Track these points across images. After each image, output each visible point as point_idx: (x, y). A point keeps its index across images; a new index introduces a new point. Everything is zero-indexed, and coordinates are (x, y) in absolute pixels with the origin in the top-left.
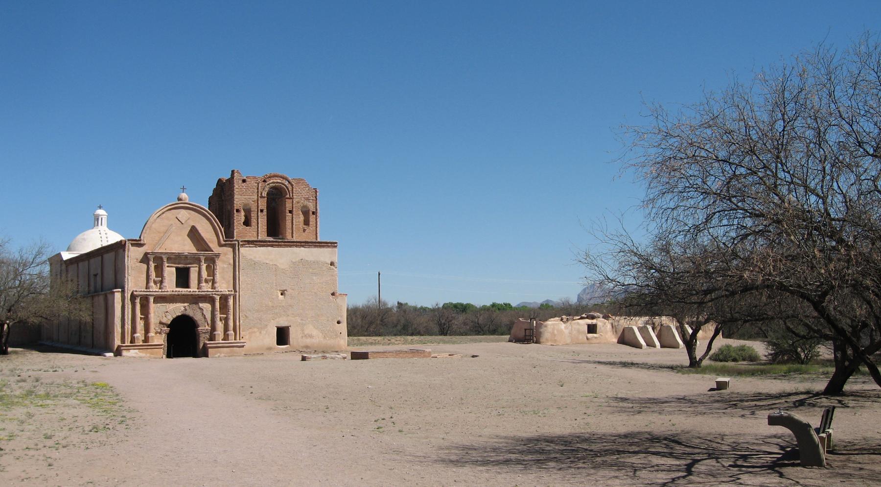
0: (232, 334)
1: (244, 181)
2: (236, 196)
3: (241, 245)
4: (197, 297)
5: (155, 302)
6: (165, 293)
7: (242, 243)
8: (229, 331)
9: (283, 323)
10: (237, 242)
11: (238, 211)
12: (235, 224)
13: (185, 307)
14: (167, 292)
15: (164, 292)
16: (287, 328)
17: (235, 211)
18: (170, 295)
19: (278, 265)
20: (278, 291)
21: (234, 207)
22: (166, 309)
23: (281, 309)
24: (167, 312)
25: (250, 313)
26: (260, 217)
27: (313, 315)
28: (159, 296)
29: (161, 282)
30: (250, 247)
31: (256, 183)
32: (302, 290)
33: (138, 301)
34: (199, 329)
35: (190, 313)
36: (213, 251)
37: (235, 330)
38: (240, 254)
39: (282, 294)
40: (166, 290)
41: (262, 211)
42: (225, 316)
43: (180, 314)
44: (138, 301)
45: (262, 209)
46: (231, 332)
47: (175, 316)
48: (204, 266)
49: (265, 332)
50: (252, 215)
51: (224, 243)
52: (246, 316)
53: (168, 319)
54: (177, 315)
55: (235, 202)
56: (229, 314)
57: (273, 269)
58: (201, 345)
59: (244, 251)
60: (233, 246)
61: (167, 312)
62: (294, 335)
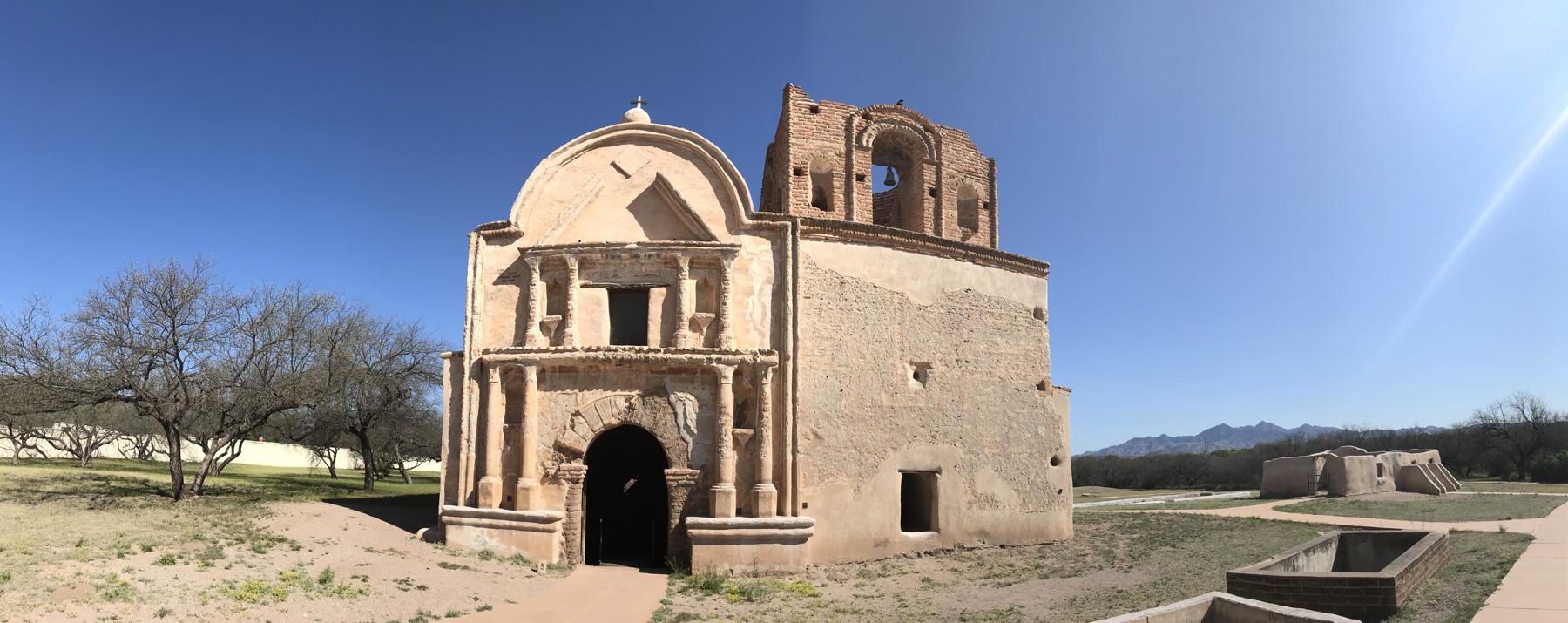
0: (771, 492)
1: (814, 110)
2: (792, 140)
3: (804, 233)
4: (664, 368)
5: (541, 380)
6: (567, 355)
7: (805, 227)
8: (760, 482)
9: (920, 460)
10: (790, 223)
11: (798, 172)
12: (790, 200)
13: (628, 399)
14: (574, 350)
15: (565, 350)
16: (932, 475)
17: (791, 171)
18: (582, 360)
19: (908, 294)
20: (907, 366)
21: (789, 161)
22: (577, 405)
23: (913, 415)
24: (577, 414)
25: (827, 425)
26: (855, 190)
27: (998, 439)
28: (557, 365)
29: (563, 325)
30: (827, 239)
31: (843, 117)
32: (971, 368)
33: (495, 376)
34: (666, 471)
35: (643, 418)
36: (716, 240)
37: (779, 480)
38: (800, 259)
39: (916, 376)
40: (569, 347)
41: (861, 178)
42: (750, 431)
43: (615, 422)
44: (495, 376)
45: (860, 172)
46: (768, 488)
47: (599, 427)
48: (689, 287)
49: (870, 489)
50: (836, 184)
51: (750, 222)
52: (816, 435)
53: (581, 438)
54: (606, 422)
55: (792, 150)
56: (761, 425)
57: (892, 303)
58: (675, 521)
59: (814, 252)
60: (778, 238)
61: (577, 414)
62: (950, 497)
